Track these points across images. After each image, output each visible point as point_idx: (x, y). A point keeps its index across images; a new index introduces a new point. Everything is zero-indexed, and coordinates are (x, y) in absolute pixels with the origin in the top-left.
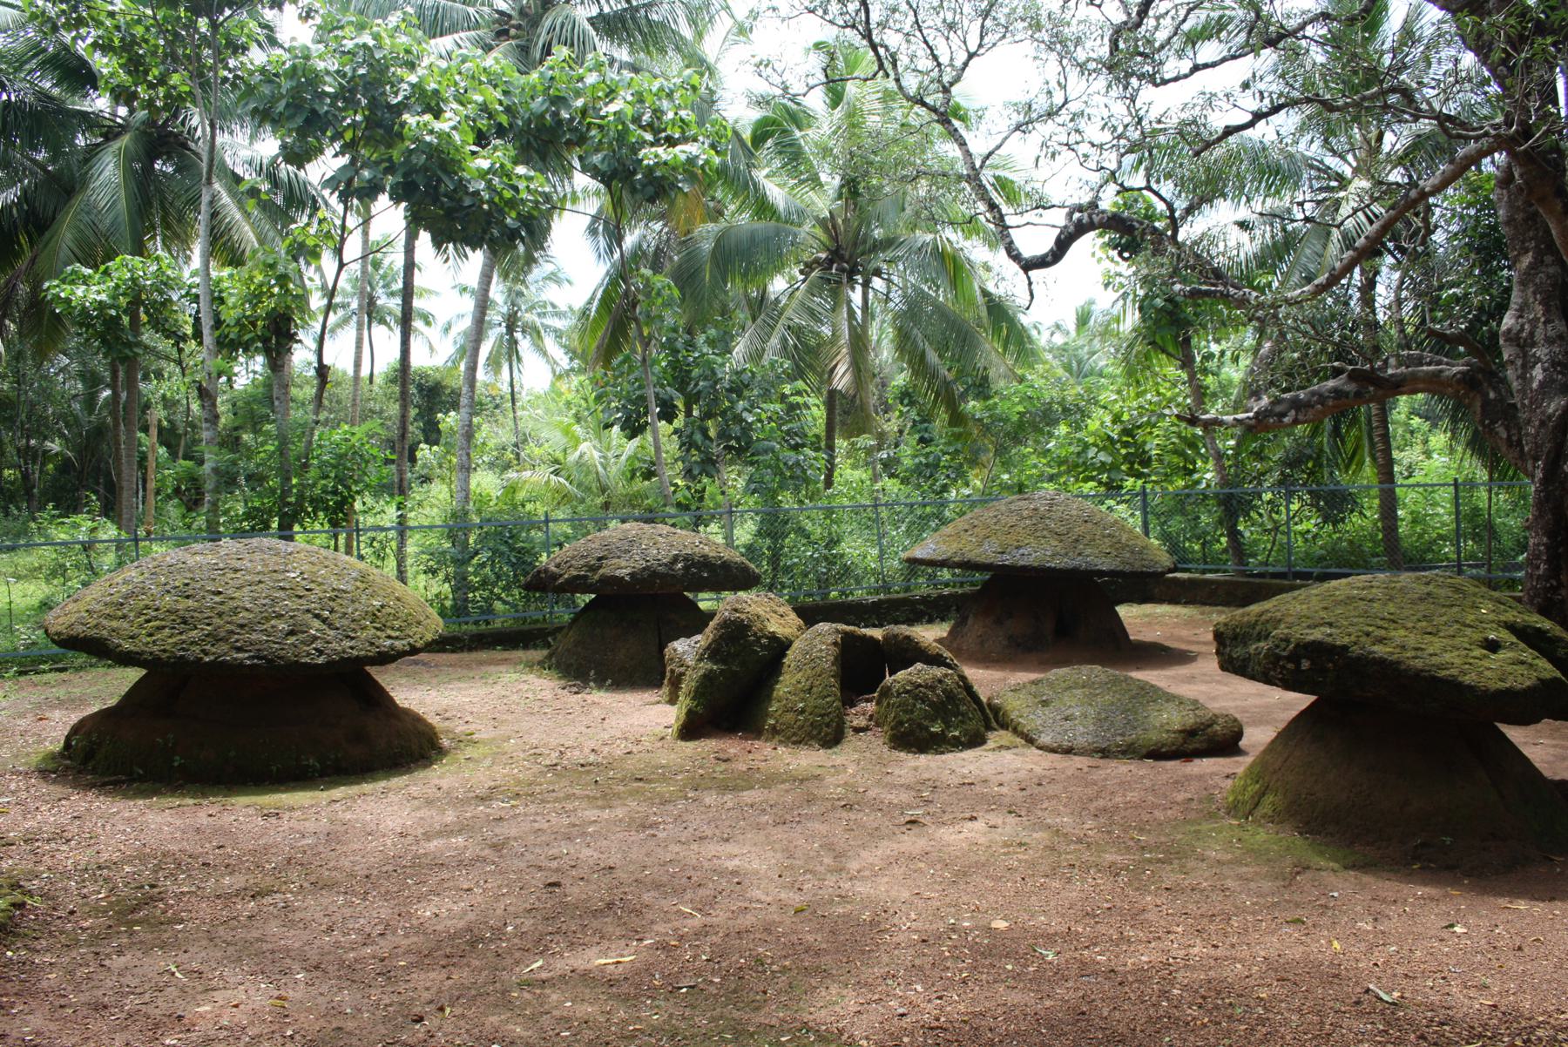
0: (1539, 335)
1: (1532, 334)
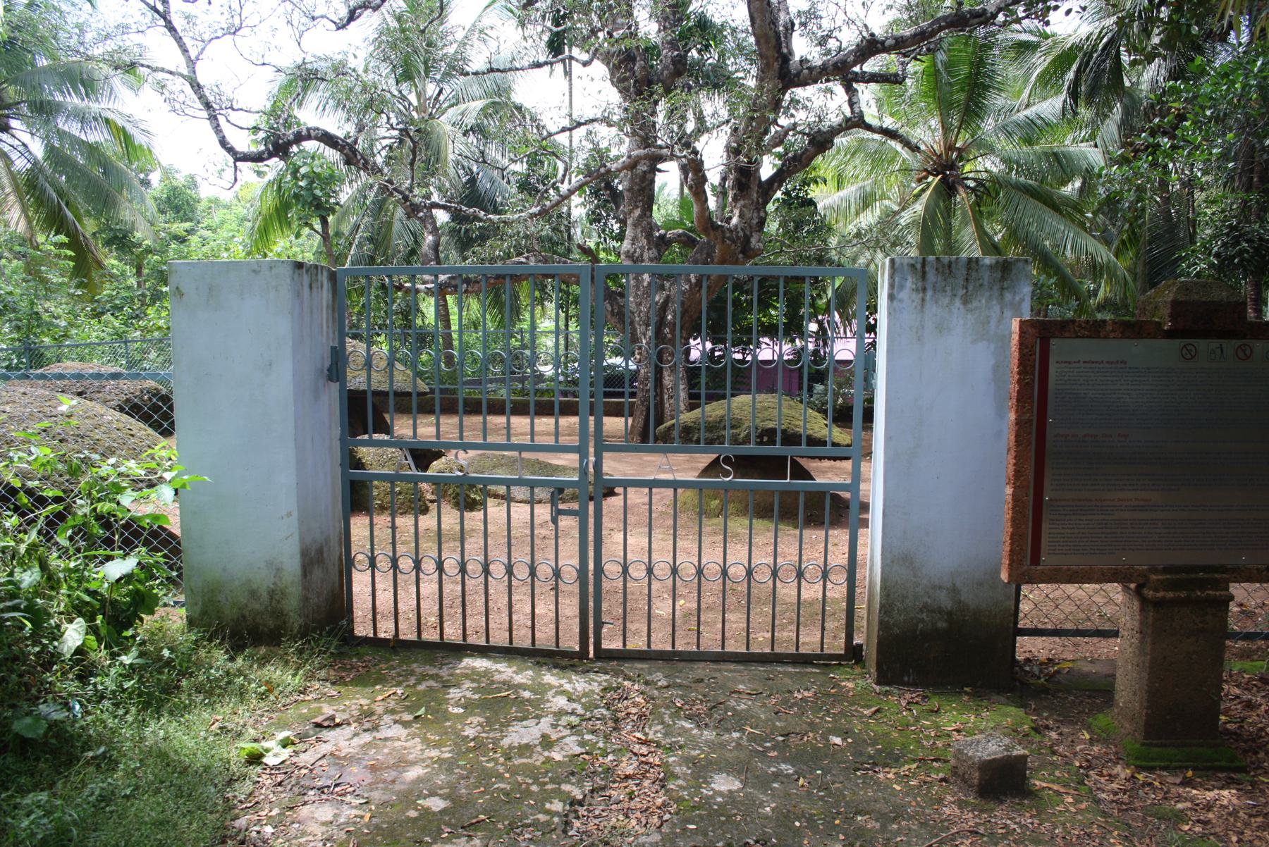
0: (646, 256)
1: (642, 255)
